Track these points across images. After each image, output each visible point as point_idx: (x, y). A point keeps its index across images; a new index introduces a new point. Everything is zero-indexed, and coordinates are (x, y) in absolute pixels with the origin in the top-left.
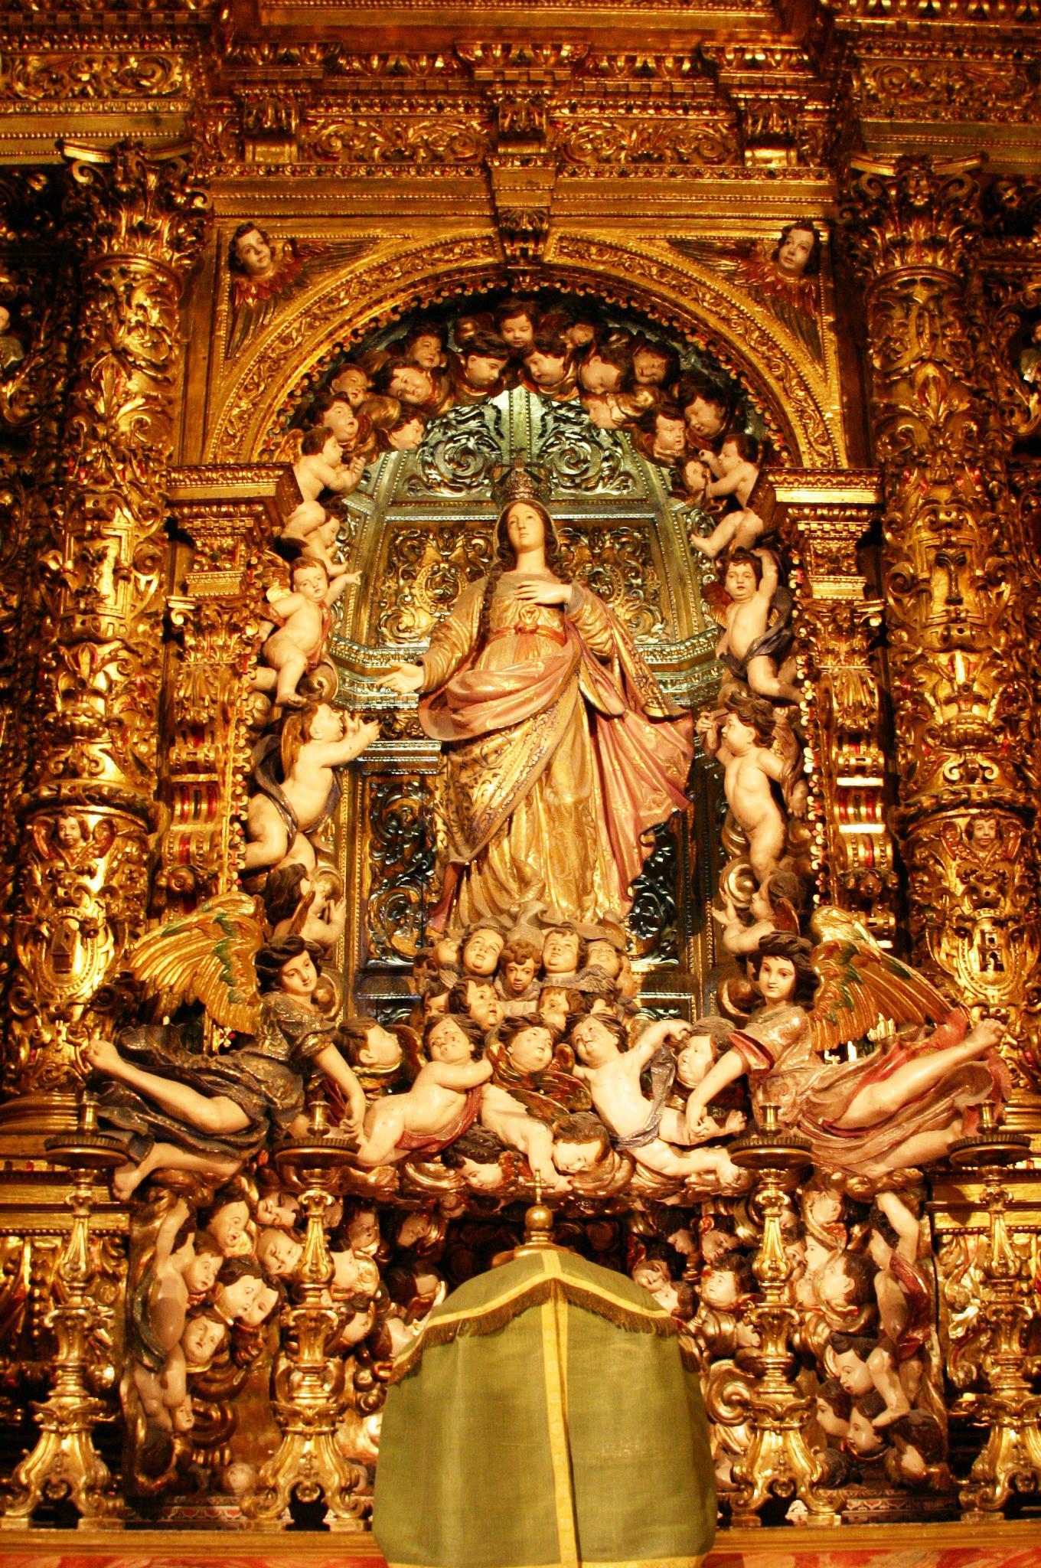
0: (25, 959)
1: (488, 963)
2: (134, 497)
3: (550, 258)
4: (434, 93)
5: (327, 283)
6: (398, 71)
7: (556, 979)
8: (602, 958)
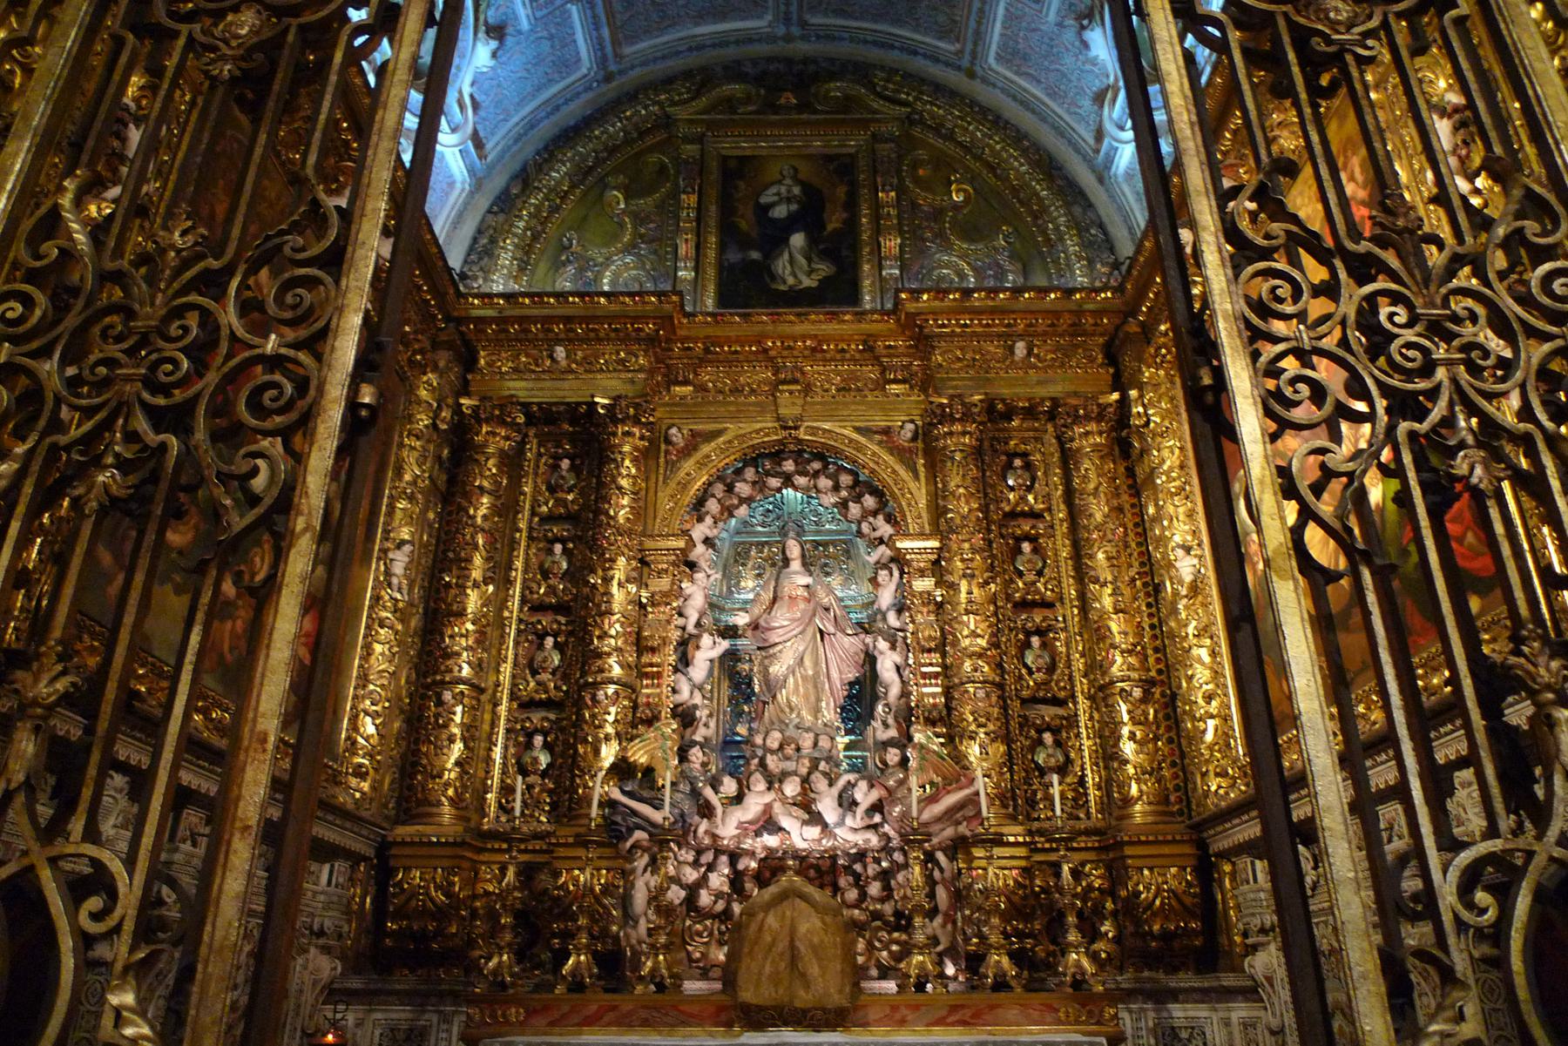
0: (581, 750)
1: (776, 745)
3: (802, 436)
5: (706, 449)
6: (736, 352)
7: (805, 752)
8: (824, 743)
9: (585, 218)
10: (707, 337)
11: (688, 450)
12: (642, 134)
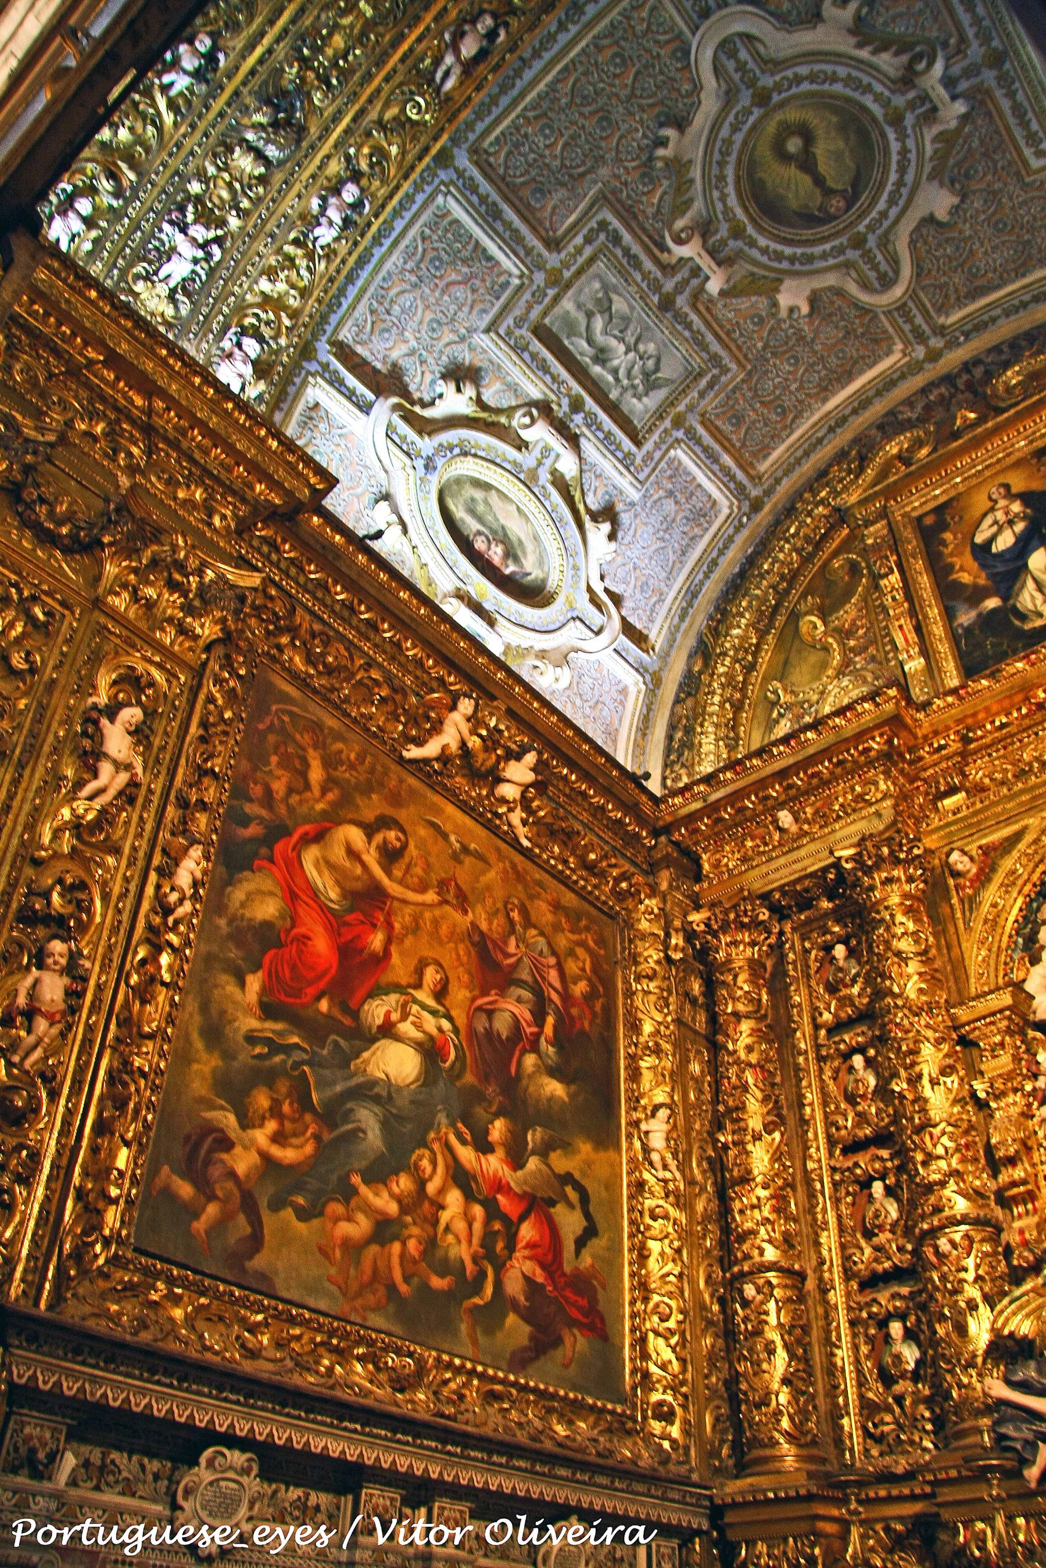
2: (929, 1033)
4: (1030, 727)
5: (1007, 863)
6: (1003, 726)
9: (786, 663)
10: (958, 722)
11: (983, 878)
12: (818, 546)
